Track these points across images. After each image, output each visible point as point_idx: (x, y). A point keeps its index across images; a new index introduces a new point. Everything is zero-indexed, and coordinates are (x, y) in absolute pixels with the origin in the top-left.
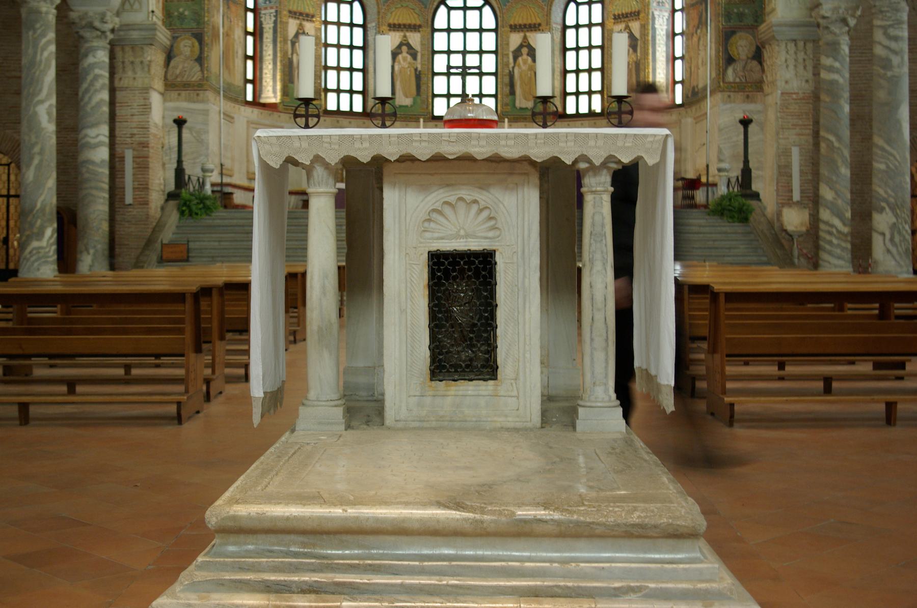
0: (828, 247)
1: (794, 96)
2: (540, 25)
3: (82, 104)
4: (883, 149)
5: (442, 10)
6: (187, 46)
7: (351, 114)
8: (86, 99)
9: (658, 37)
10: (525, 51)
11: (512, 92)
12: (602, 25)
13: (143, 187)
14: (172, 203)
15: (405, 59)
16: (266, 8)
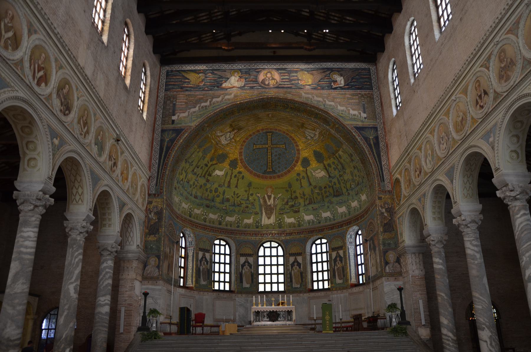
0: (448, 347)
1: (417, 277)
2: (301, 253)
3: (99, 285)
4: (479, 298)
5: (262, 248)
6: (153, 261)
7: (224, 291)
8: (101, 283)
9: (351, 256)
10: (296, 264)
11: (291, 281)
12: (327, 252)
13: (128, 325)
14: (139, 332)
15: (247, 268)
16: (190, 247)
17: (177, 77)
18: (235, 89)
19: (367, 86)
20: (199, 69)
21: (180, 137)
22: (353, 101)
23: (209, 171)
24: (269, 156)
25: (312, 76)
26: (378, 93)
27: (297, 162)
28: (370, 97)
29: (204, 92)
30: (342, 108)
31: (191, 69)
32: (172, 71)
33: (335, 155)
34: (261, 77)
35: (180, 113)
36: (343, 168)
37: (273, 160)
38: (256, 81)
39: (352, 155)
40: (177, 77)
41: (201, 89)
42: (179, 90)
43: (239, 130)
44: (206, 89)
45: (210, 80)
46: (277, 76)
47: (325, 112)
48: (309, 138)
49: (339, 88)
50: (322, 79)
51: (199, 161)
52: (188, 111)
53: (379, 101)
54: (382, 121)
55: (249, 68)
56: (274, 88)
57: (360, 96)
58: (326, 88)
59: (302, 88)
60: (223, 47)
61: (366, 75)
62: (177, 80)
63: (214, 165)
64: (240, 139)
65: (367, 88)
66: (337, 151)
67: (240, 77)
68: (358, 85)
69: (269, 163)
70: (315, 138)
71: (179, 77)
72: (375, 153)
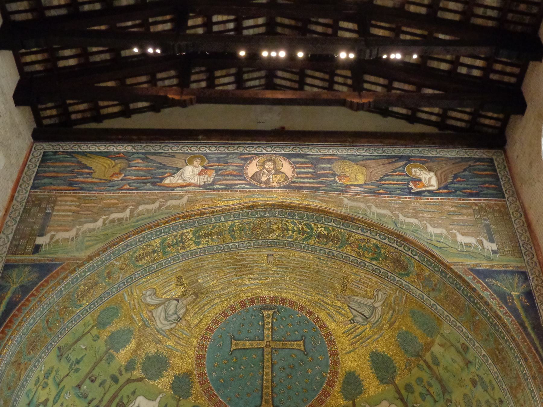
17: (65, 164)
18: (191, 188)
19: (490, 192)
20: (115, 150)
21: (47, 281)
22: (461, 218)
23: (120, 395)
24: (266, 371)
25: (364, 170)
26: (518, 203)
27: (331, 384)
28: (500, 212)
29: (120, 193)
30: (438, 231)
31: (98, 150)
32: (55, 153)
33: (421, 357)
34: (252, 169)
35: (57, 231)
36: (445, 390)
37: (276, 380)
38: (240, 175)
39: (466, 348)
40: (65, 164)
41: (116, 188)
42: (66, 187)
43: (197, 296)
44: (128, 187)
45: (138, 170)
46: (286, 168)
48: (359, 319)
49: (426, 193)
50: (387, 175)
51: (96, 364)
52: (78, 227)
53: (523, 218)
54: (535, 259)
55: (227, 151)
57: (476, 208)
58: (398, 192)
59: (342, 191)
60: (170, 96)
61: (485, 170)
62: (63, 169)
63: (134, 381)
64: (201, 321)
65: (492, 194)
66: (428, 347)
67: (206, 168)
68: (471, 189)
69: (267, 387)
70: (373, 320)
71: (68, 164)
72: (529, 329)
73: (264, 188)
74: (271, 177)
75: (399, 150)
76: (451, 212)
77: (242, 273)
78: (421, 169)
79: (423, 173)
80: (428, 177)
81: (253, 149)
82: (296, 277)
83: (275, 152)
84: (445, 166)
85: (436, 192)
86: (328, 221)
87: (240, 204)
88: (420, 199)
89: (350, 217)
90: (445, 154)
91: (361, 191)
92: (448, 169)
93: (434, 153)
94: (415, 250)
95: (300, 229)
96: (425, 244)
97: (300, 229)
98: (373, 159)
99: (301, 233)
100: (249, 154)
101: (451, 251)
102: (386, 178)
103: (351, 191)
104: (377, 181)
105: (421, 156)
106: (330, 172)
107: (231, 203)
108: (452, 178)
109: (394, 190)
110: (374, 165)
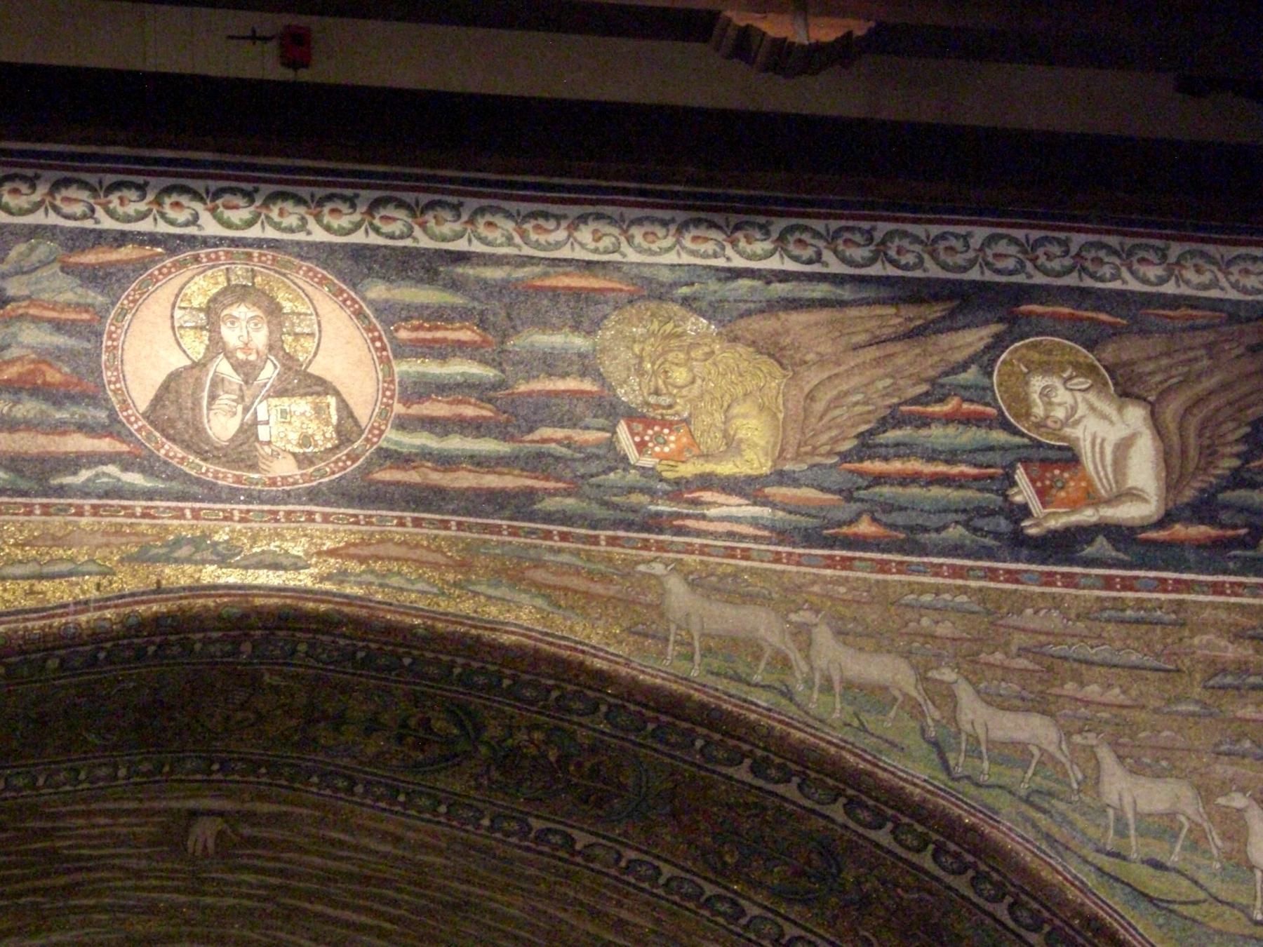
25: (772, 380)
47: (951, 827)
49: (1101, 541)
50: (893, 419)
56: (314, 495)
58: (956, 533)
73: (232, 495)
74: (262, 411)
75: (958, 245)
76: (1224, 671)
77: (28, 884)
78: (1082, 382)
79: (1092, 408)
80: (1112, 435)
81: (142, 206)
82: (330, 911)
83: (271, 233)
84: (1206, 362)
85: (1153, 535)
86: (577, 705)
87: (102, 604)
88: (1070, 581)
89: (703, 706)
90: (1206, 278)
91: (755, 522)
92: (1224, 387)
93: (1153, 272)
94: (1035, 906)
95: (413, 722)
96: (1091, 880)
97: (413, 722)
98: (824, 303)
99: (410, 740)
100: (121, 239)
101: (1216, 925)
102: (893, 435)
103: (703, 525)
104: (845, 457)
105: (1084, 292)
106: (587, 385)
107: (56, 592)
108: (1242, 448)
109: (935, 521)
110: (826, 348)
